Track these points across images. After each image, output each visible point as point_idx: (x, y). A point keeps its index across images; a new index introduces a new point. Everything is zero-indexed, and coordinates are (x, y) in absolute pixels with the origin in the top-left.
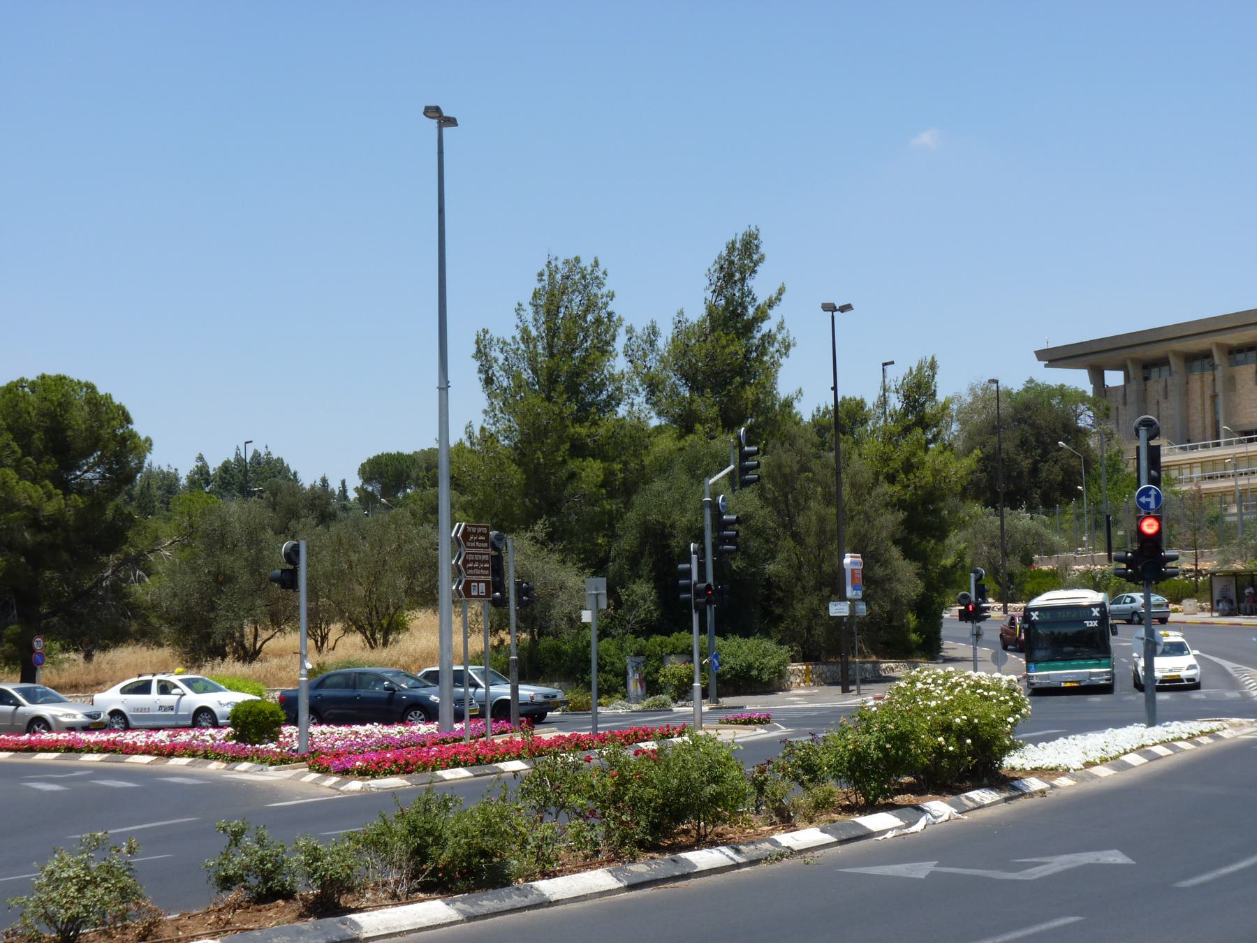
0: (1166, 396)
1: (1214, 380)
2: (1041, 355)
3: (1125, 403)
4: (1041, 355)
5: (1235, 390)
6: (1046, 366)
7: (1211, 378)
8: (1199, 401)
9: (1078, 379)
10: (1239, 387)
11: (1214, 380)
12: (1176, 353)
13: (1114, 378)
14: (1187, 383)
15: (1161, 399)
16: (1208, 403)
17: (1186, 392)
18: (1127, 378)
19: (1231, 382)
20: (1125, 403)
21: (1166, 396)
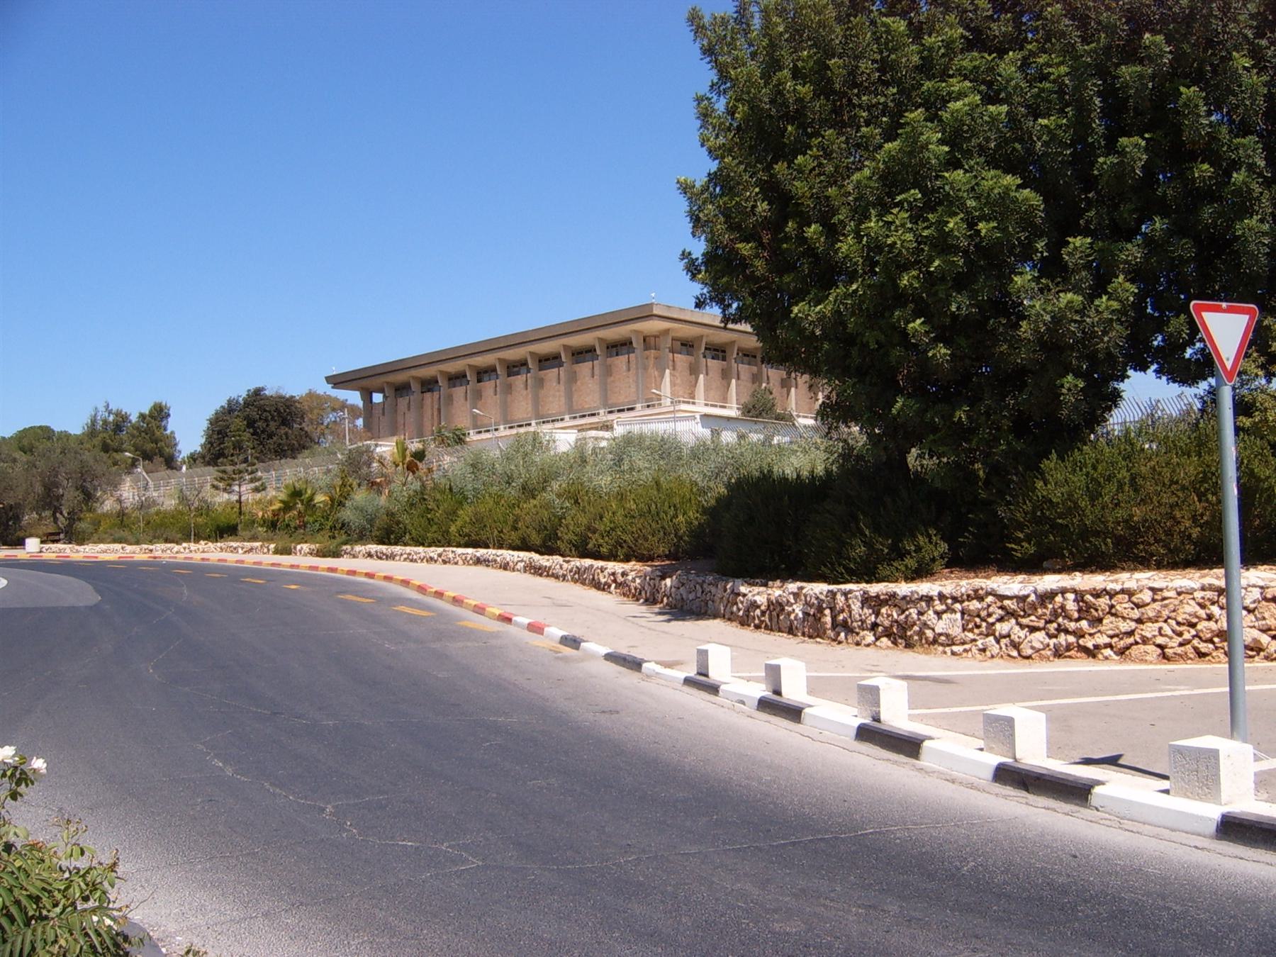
0: (409, 410)
1: (440, 398)
2: (329, 379)
3: (383, 414)
4: (329, 379)
5: (452, 404)
6: (333, 388)
7: (438, 396)
8: (429, 412)
9: (354, 398)
10: (455, 402)
11: (440, 398)
12: (414, 378)
13: (378, 398)
14: (423, 400)
15: (406, 412)
16: (435, 414)
17: (421, 406)
18: (385, 397)
19: (450, 398)
20: (383, 414)
21: (409, 410)
